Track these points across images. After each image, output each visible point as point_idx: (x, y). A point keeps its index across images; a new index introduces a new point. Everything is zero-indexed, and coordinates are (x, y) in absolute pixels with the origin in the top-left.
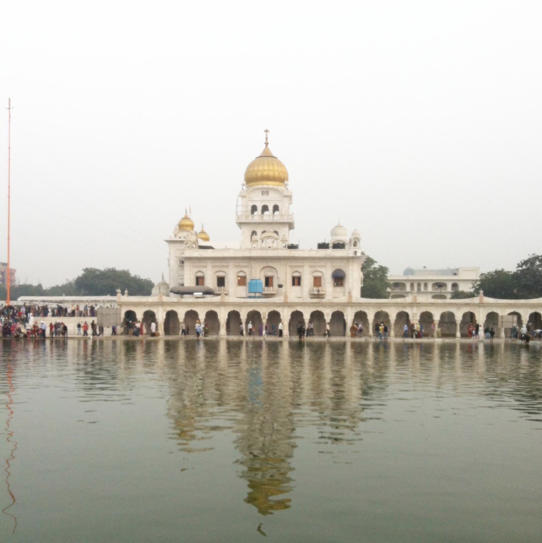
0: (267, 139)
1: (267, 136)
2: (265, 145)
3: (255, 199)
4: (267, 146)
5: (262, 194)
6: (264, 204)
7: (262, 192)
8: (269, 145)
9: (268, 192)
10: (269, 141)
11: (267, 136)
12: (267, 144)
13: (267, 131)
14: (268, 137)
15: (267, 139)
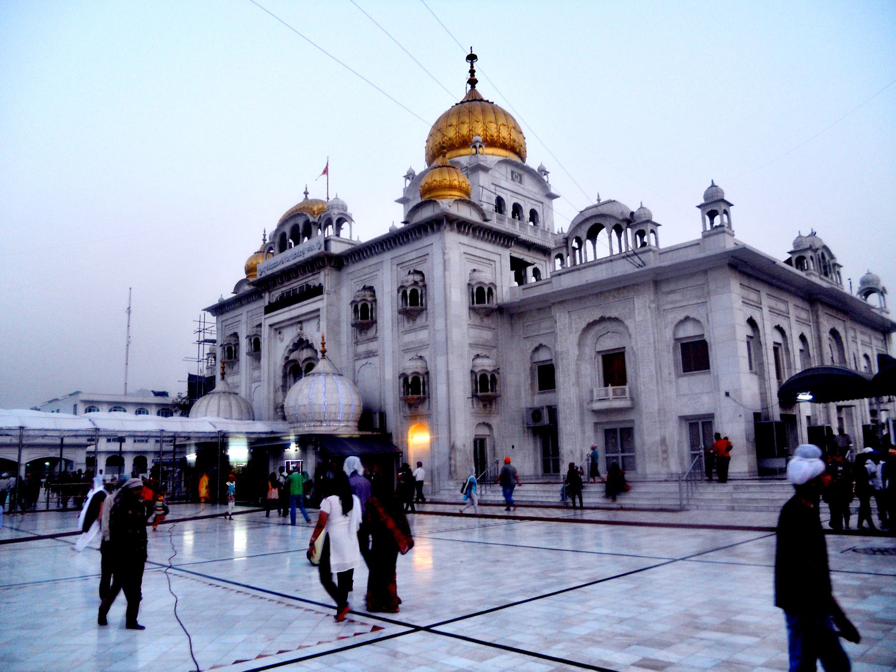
0: (472, 72)
1: (472, 66)
2: (469, 86)
3: (503, 184)
4: (473, 87)
5: (513, 179)
6: (516, 201)
7: (512, 173)
8: (477, 86)
9: (520, 176)
10: (477, 76)
11: (472, 66)
12: (473, 82)
13: (472, 58)
14: (475, 68)
15: (472, 72)
